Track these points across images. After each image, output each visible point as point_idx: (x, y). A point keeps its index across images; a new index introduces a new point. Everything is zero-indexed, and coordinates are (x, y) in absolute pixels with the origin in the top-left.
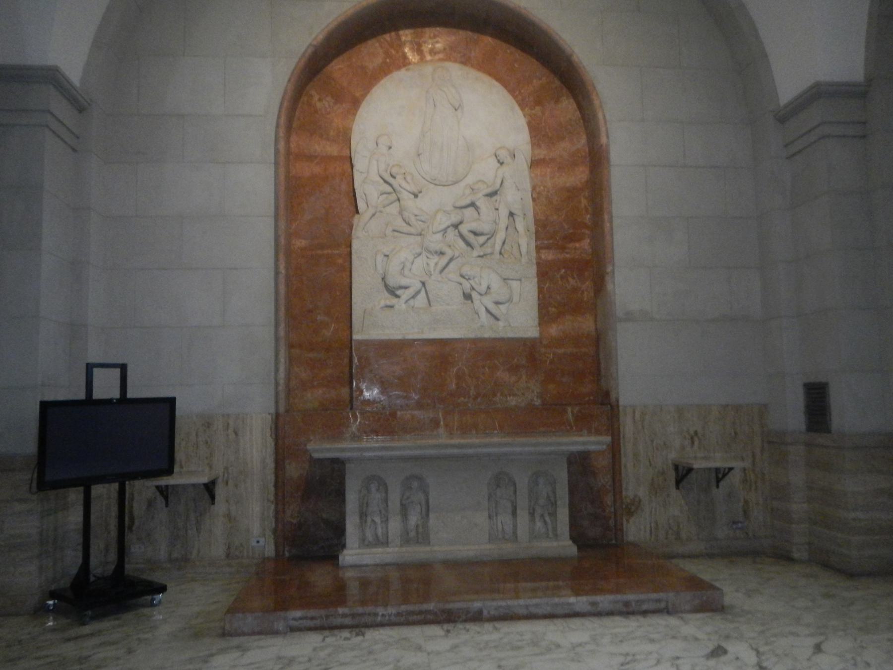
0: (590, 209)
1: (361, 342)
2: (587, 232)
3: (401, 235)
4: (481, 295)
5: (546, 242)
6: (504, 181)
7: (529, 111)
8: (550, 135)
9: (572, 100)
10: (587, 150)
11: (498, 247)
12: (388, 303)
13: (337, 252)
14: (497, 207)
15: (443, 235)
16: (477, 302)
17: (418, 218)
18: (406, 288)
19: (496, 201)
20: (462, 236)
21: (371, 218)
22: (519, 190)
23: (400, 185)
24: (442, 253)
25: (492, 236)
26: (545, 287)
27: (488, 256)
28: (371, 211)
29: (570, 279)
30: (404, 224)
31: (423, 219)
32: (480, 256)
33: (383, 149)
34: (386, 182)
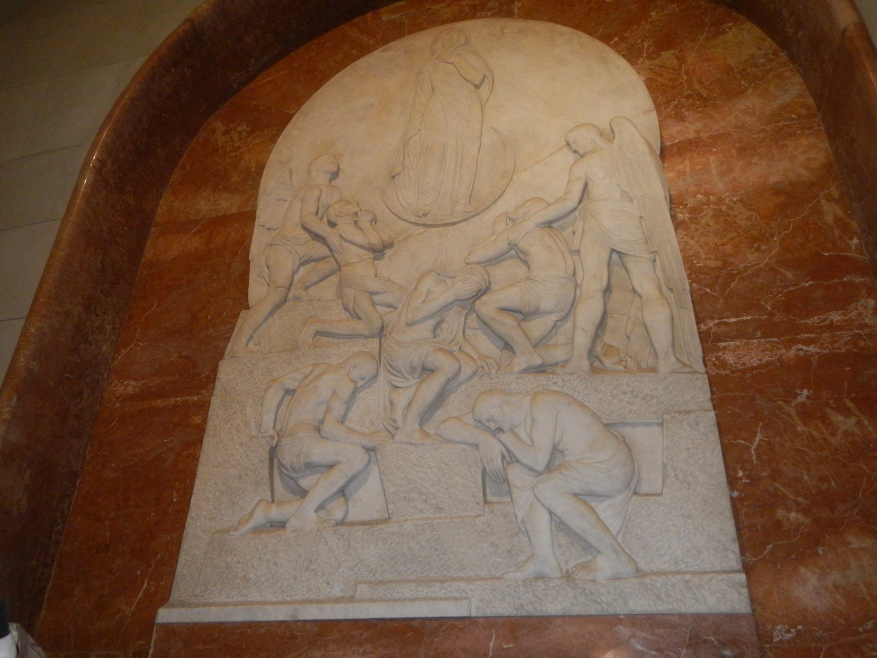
0: (854, 224)
1: (170, 630)
2: (858, 279)
3: (335, 341)
4: (539, 474)
5: (733, 320)
6: (590, 184)
7: (647, 62)
8: (705, 93)
9: (748, 25)
10: (811, 101)
11: (582, 340)
12: (275, 513)
13: (196, 398)
14: (576, 245)
15: (438, 325)
16: (523, 498)
17: (376, 298)
19: (574, 233)
21: (272, 313)
22: (632, 200)
23: (341, 237)
24: (427, 371)
25: (566, 316)
26: (754, 447)
27: (558, 370)
28: (275, 297)
29: (837, 418)
30: (345, 315)
31: (390, 299)
32: (540, 370)
33: (322, 179)
34: (317, 237)
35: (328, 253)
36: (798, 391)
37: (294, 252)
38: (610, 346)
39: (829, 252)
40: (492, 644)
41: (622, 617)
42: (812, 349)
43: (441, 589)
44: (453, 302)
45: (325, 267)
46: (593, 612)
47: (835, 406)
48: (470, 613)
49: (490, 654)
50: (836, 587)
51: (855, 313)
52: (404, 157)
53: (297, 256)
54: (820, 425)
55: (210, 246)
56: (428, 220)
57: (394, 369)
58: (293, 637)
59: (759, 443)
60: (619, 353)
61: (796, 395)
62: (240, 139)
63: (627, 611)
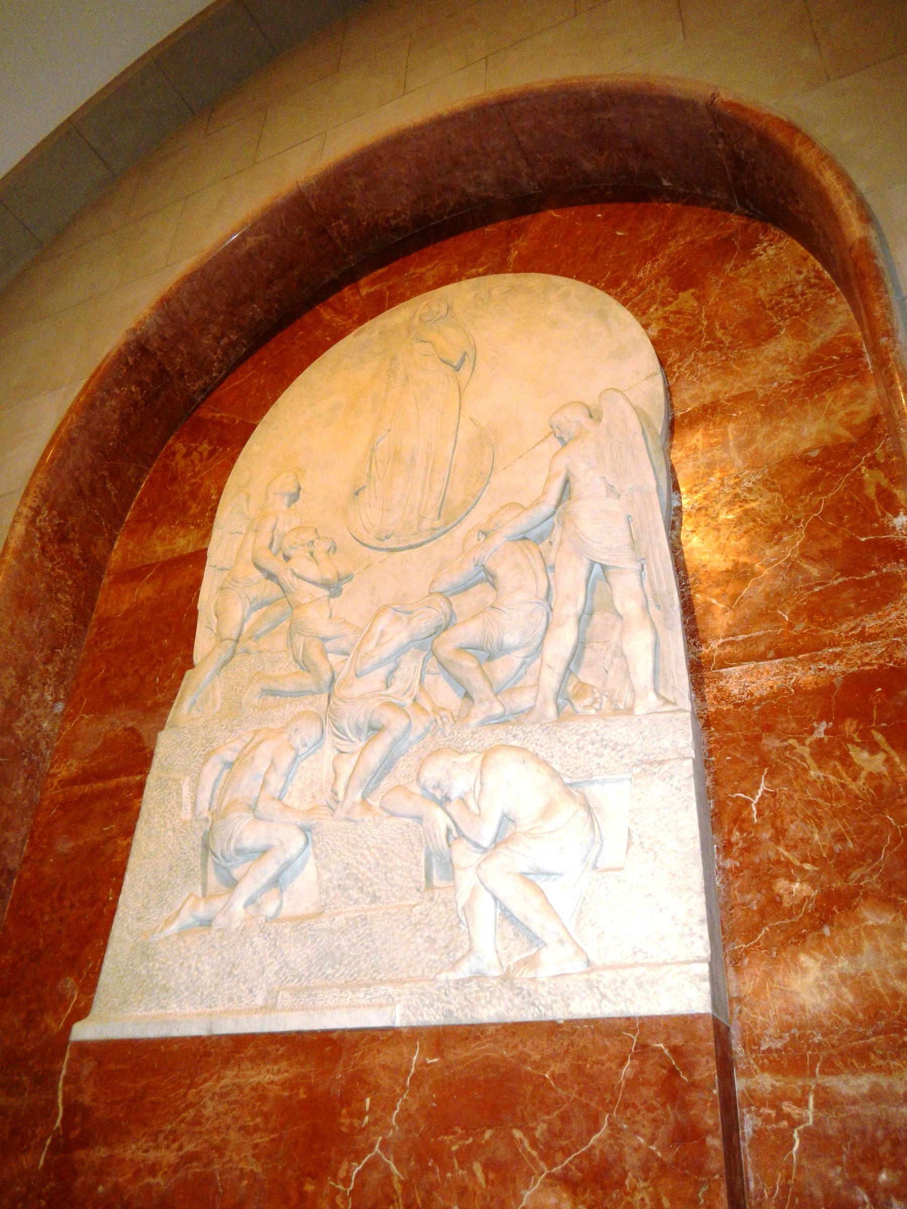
1: (84, 1048)
3: (282, 700)
4: (485, 850)
6: (572, 480)
9: (787, 241)
11: (550, 680)
16: (466, 880)
17: (329, 645)
18: (264, 851)
20: (443, 666)
23: (294, 574)
29: (860, 756)
30: (294, 668)
31: (344, 645)
32: (502, 721)
34: (271, 576)
35: (281, 594)
36: (815, 724)
37: (243, 596)
38: (584, 684)
39: (866, 535)
40: (415, 1058)
41: (562, 1022)
42: (837, 667)
43: (366, 994)
44: (408, 644)
45: (276, 611)
46: (530, 1019)
47: (859, 741)
48: (394, 1022)
49: (413, 1070)
50: (843, 977)
51: (894, 615)
52: (370, 465)
53: (247, 601)
54: (839, 767)
55: (163, 595)
56: (391, 543)
57: (339, 731)
58: (207, 1054)
59: (762, 796)
60: (593, 693)
61: (811, 732)
62: (201, 460)
63: (566, 1016)
